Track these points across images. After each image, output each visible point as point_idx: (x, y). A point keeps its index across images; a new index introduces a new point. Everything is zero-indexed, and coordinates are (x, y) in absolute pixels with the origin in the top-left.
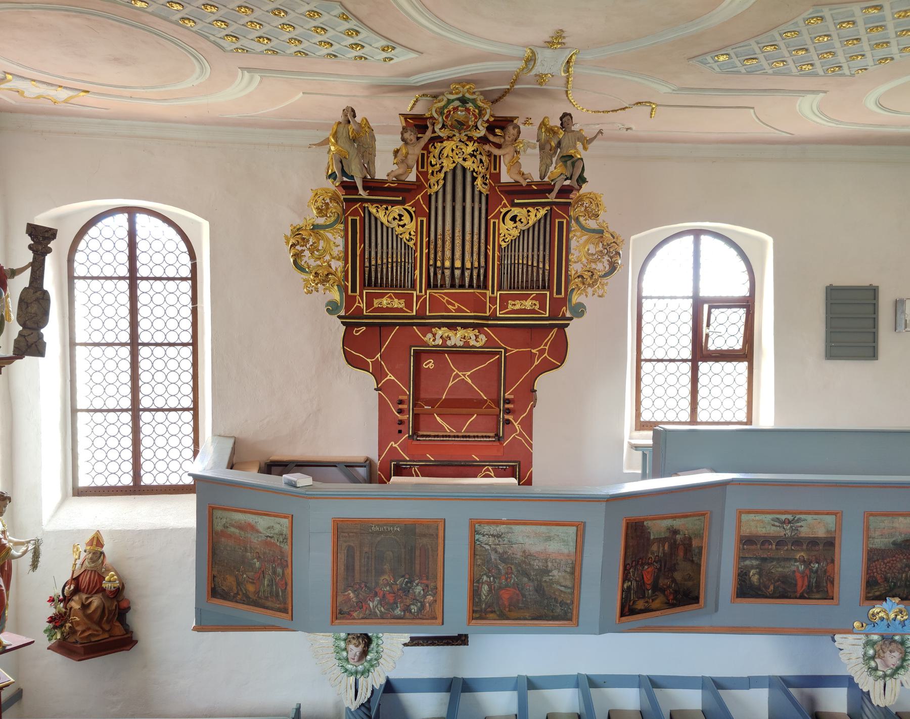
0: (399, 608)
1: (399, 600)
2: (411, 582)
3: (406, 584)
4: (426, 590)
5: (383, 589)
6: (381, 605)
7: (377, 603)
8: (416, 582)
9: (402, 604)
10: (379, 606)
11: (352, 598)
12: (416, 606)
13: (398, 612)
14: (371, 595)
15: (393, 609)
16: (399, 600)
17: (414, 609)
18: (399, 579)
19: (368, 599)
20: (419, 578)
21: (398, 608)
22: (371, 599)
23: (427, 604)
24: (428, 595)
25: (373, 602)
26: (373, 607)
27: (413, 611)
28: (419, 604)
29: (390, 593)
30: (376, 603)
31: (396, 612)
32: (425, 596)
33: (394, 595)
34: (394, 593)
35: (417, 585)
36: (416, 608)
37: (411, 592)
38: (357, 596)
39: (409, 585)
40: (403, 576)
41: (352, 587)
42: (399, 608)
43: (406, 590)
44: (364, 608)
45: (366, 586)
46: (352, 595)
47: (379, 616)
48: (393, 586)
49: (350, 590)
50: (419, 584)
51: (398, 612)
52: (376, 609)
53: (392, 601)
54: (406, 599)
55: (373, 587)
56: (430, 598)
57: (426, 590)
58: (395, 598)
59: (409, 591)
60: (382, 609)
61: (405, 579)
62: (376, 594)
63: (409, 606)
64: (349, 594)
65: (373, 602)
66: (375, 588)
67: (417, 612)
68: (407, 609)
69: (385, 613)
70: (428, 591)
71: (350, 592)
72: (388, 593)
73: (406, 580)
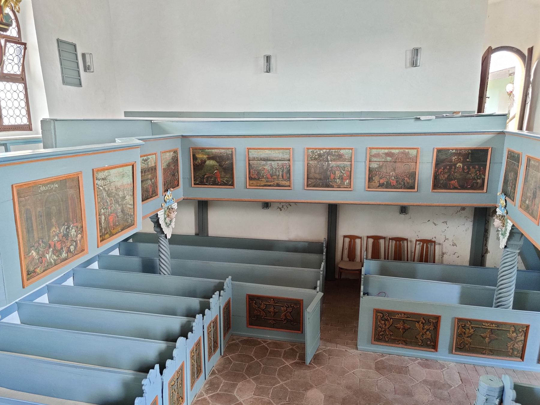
0: (64, 252)
1: (64, 245)
2: (68, 228)
3: (66, 231)
4: (77, 231)
5: (53, 240)
6: (54, 254)
7: (51, 253)
8: (71, 226)
9: (66, 247)
10: (53, 255)
11: (35, 257)
12: (73, 245)
13: (64, 255)
14: (46, 249)
15: (61, 254)
16: (64, 245)
17: (72, 248)
18: (62, 228)
19: (45, 253)
20: (73, 223)
21: (64, 252)
22: (47, 252)
23: (79, 242)
24: (78, 234)
25: (48, 254)
26: (49, 258)
27: (72, 250)
28: (74, 243)
29: (58, 241)
30: (50, 253)
31: (63, 256)
32: (77, 236)
33: (60, 242)
34: (61, 241)
35: (72, 228)
36: (73, 248)
37: (69, 235)
38: (38, 253)
39: (68, 230)
40: (64, 225)
41: (34, 246)
42: (64, 252)
43: (66, 236)
44: (44, 261)
45: (42, 242)
46: (34, 254)
47: (53, 264)
48: (59, 235)
49: (33, 250)
50: (73, 228)
51: (64, 255)
52: (51, 259)
53: (59, 248)
54: (67, 242)
55: (47, 241)
56: (79, 236)
57: (77, 231)
58: (62, 245)
59: (68, 235)
60: (55, 257)
61: (65, 227)
62: (50, 247)
63: (69, 248)
64: (32, 254)
65: (48, 254)
66: (49, 241)
67: (74, 250)
68: (69, 251)
69: (57, 260)
70: (78, 231)
71: (33, 251)
72: (57, 242)
73: (66, 227)
